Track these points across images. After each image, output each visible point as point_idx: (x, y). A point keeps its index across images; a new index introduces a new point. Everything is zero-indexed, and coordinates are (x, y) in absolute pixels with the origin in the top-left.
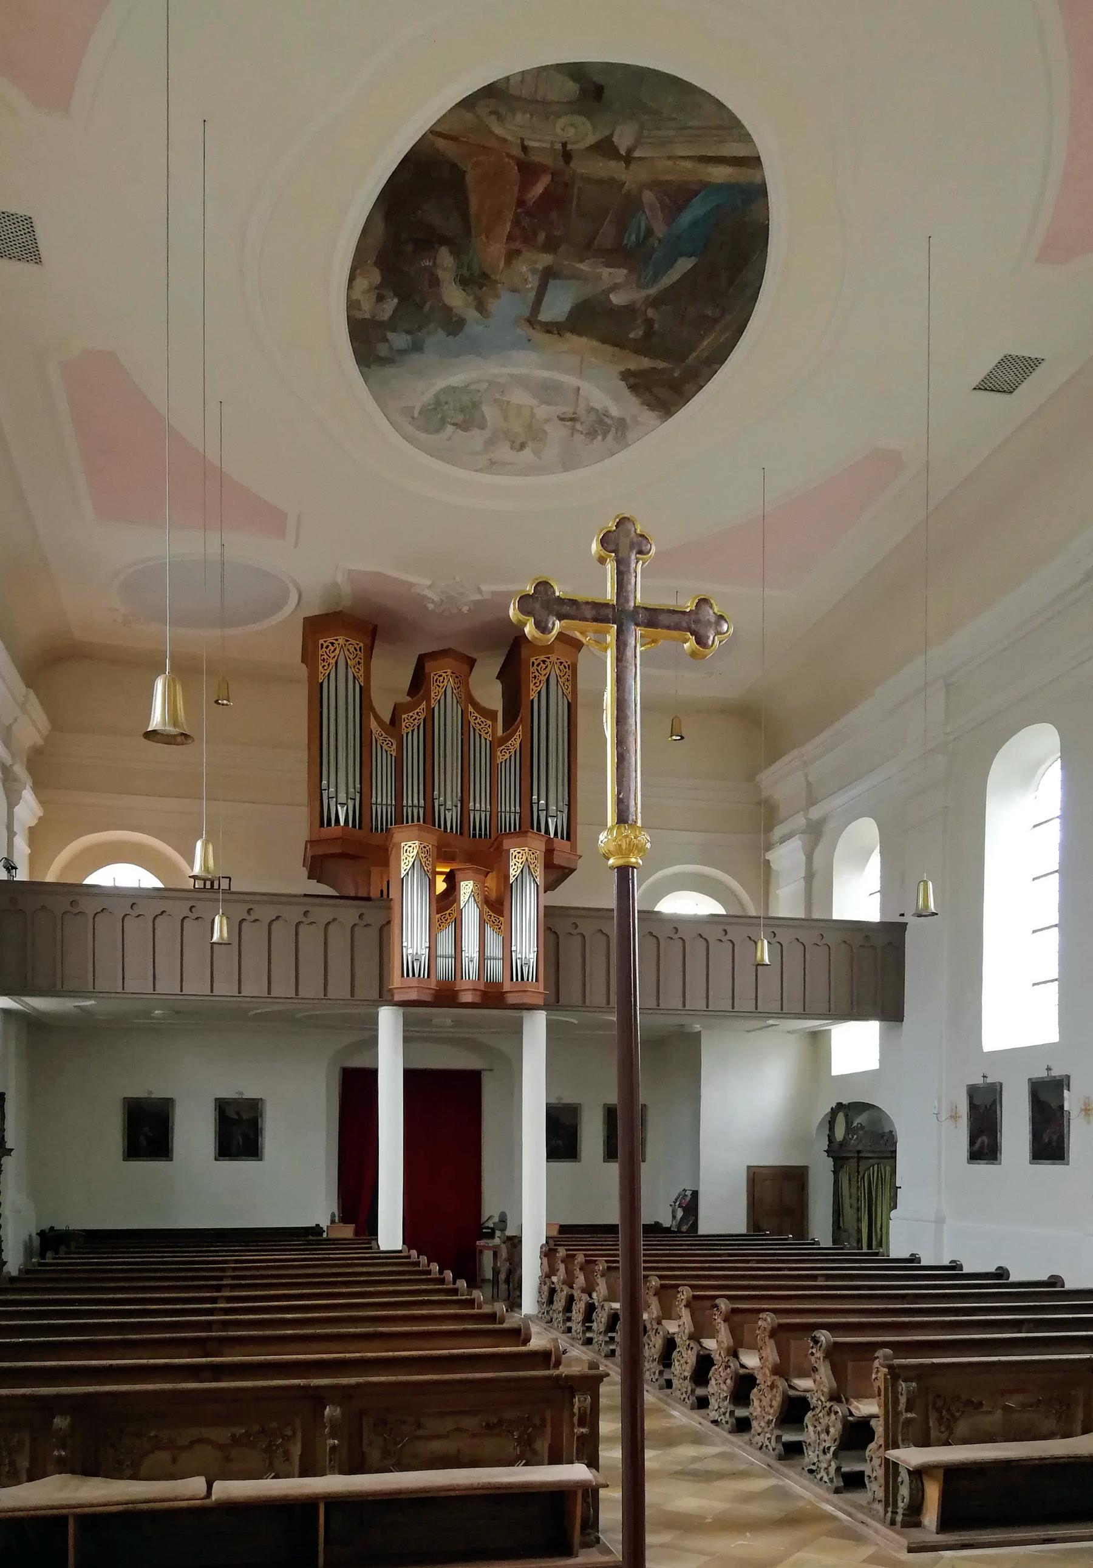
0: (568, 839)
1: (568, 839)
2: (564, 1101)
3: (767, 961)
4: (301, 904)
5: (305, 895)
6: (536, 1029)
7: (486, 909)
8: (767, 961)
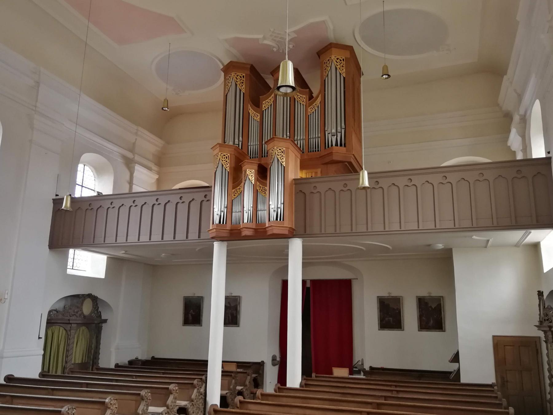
0: (345, 146)
1: (345, 146)
2: (393, 295)
3: (367, 184)
4: (178, 193)
5: (180, 189)
6: (296, 248)
7: (258, 183)
8: (367, 184)
